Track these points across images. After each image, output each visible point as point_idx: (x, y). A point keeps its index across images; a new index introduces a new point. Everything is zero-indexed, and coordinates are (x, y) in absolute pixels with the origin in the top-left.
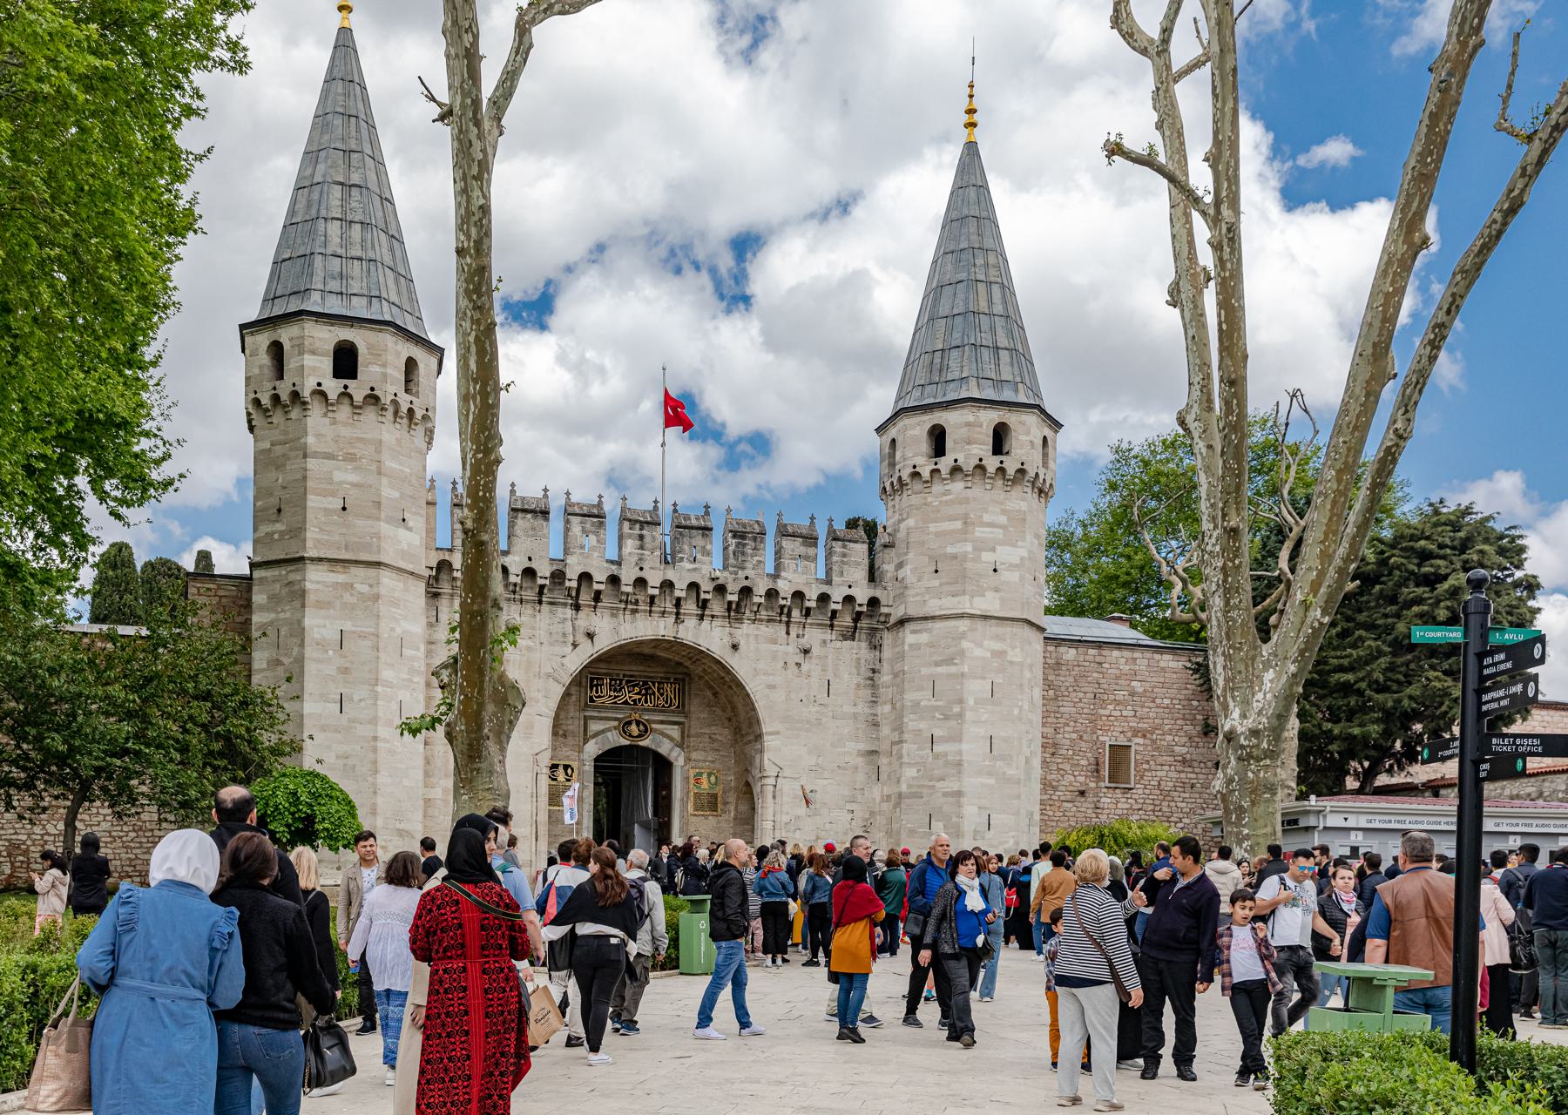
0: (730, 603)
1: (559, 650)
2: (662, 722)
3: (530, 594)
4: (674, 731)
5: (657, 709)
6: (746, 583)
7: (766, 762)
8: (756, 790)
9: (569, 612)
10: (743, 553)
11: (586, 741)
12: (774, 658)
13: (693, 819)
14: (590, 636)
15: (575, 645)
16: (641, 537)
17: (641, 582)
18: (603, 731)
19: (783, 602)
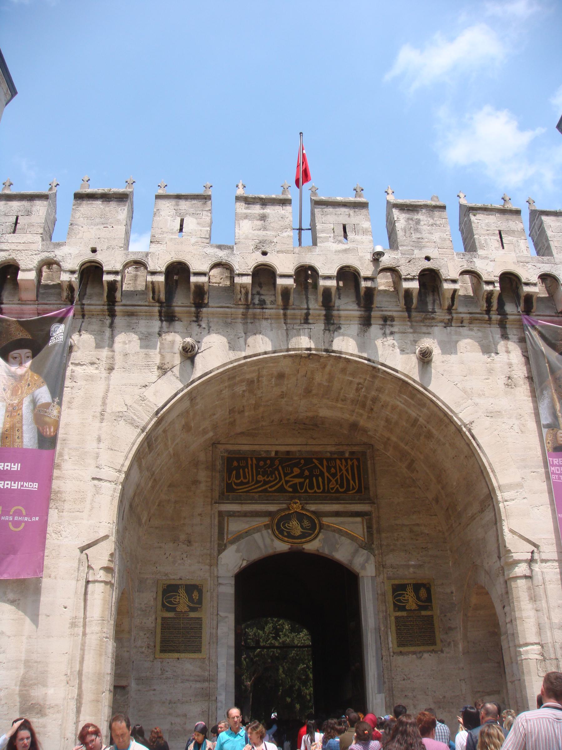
0: (408, 292)
1: (138, 377)
2: (337, 514)
3: (96, 303)
4: (356, 527)
5: (329, 495)
6: (428, 265)
7: (508, 537)
8: (496, 591)
9: (157, 323)
10: (417, 230)
11: (222, 548)
12: (490, 371)
13: (399, 660)
14: (189, 354)
15: (163, 370)
16: (263, 218)
17: (264, 274)
18: (248, 533)
19: (490, 288)
